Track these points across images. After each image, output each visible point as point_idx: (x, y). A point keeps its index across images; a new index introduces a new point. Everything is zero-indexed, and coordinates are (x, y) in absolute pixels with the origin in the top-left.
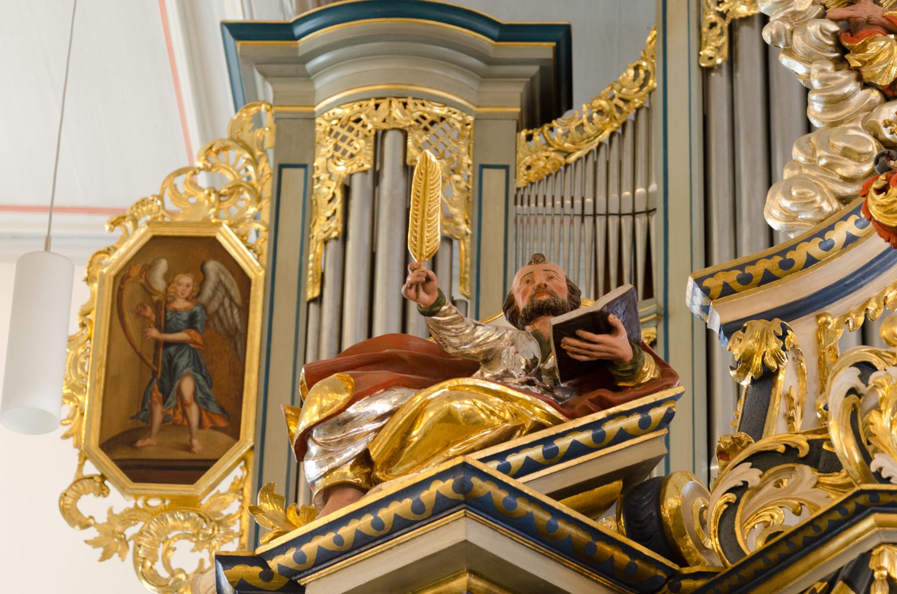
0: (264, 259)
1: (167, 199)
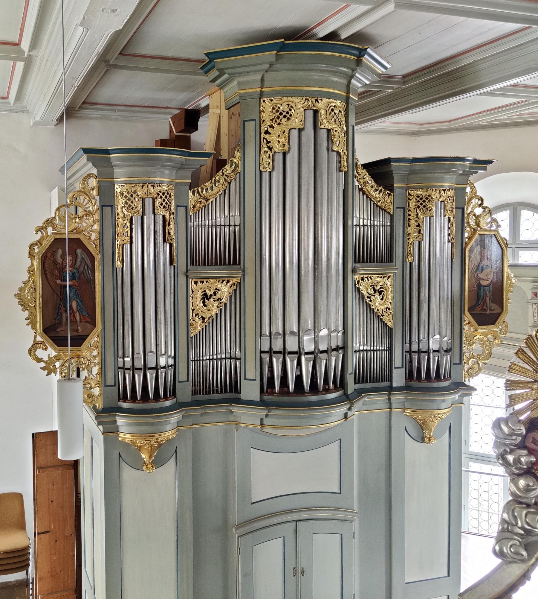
1: (57, 218)
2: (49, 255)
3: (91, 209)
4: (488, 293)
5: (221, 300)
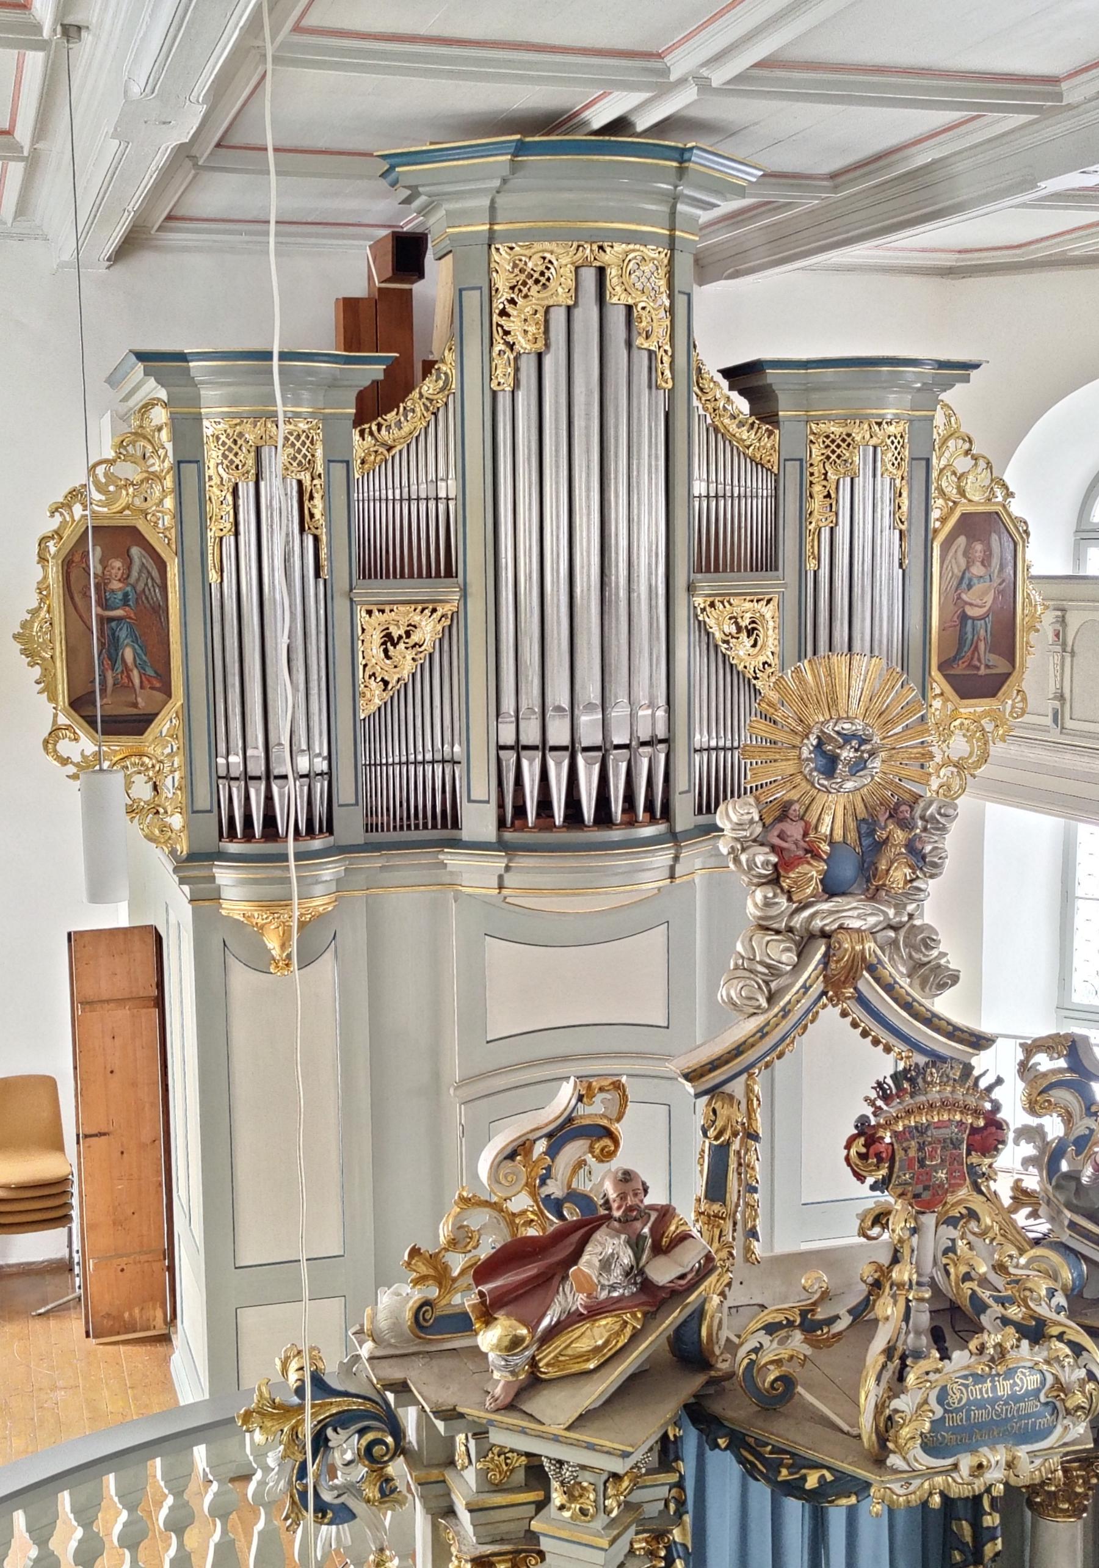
2: (77, 558)
3: (156, 468)
4: (982, 632)
5: (420, 646)
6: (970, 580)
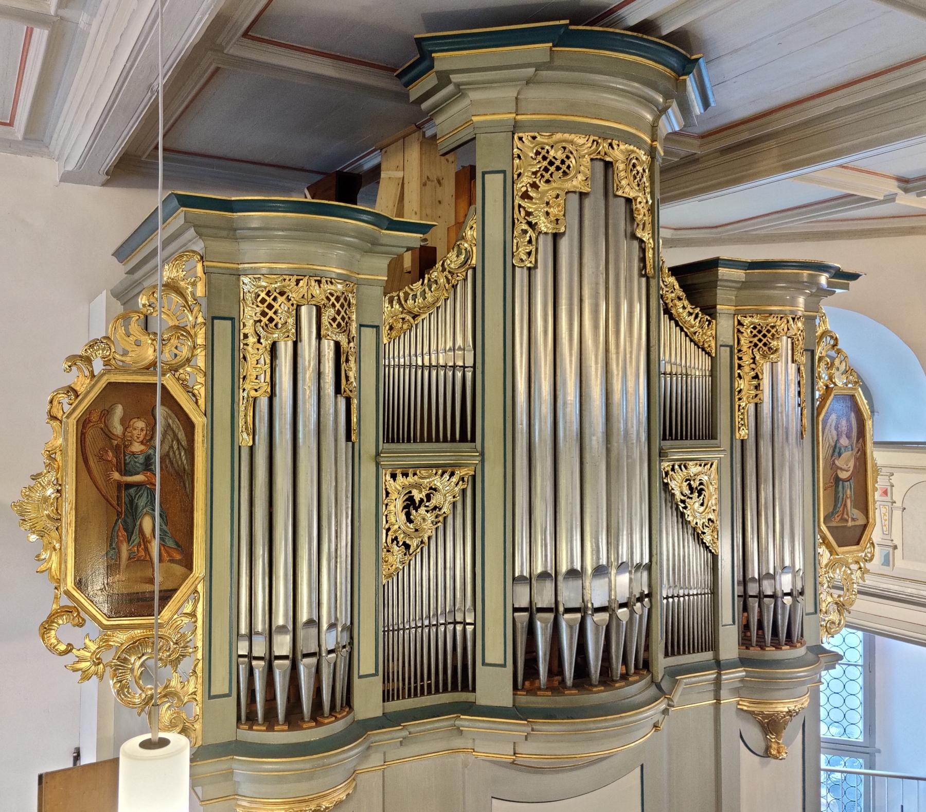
0: (202, 402)
5: (440, 509)
6: (840, 450)
